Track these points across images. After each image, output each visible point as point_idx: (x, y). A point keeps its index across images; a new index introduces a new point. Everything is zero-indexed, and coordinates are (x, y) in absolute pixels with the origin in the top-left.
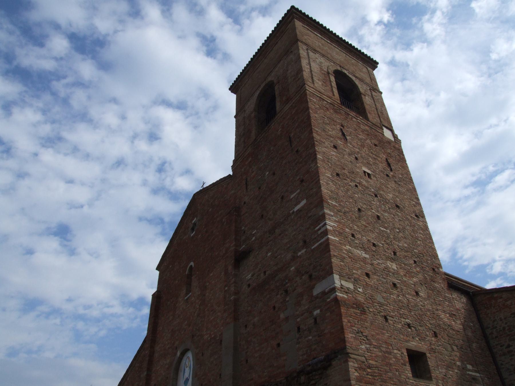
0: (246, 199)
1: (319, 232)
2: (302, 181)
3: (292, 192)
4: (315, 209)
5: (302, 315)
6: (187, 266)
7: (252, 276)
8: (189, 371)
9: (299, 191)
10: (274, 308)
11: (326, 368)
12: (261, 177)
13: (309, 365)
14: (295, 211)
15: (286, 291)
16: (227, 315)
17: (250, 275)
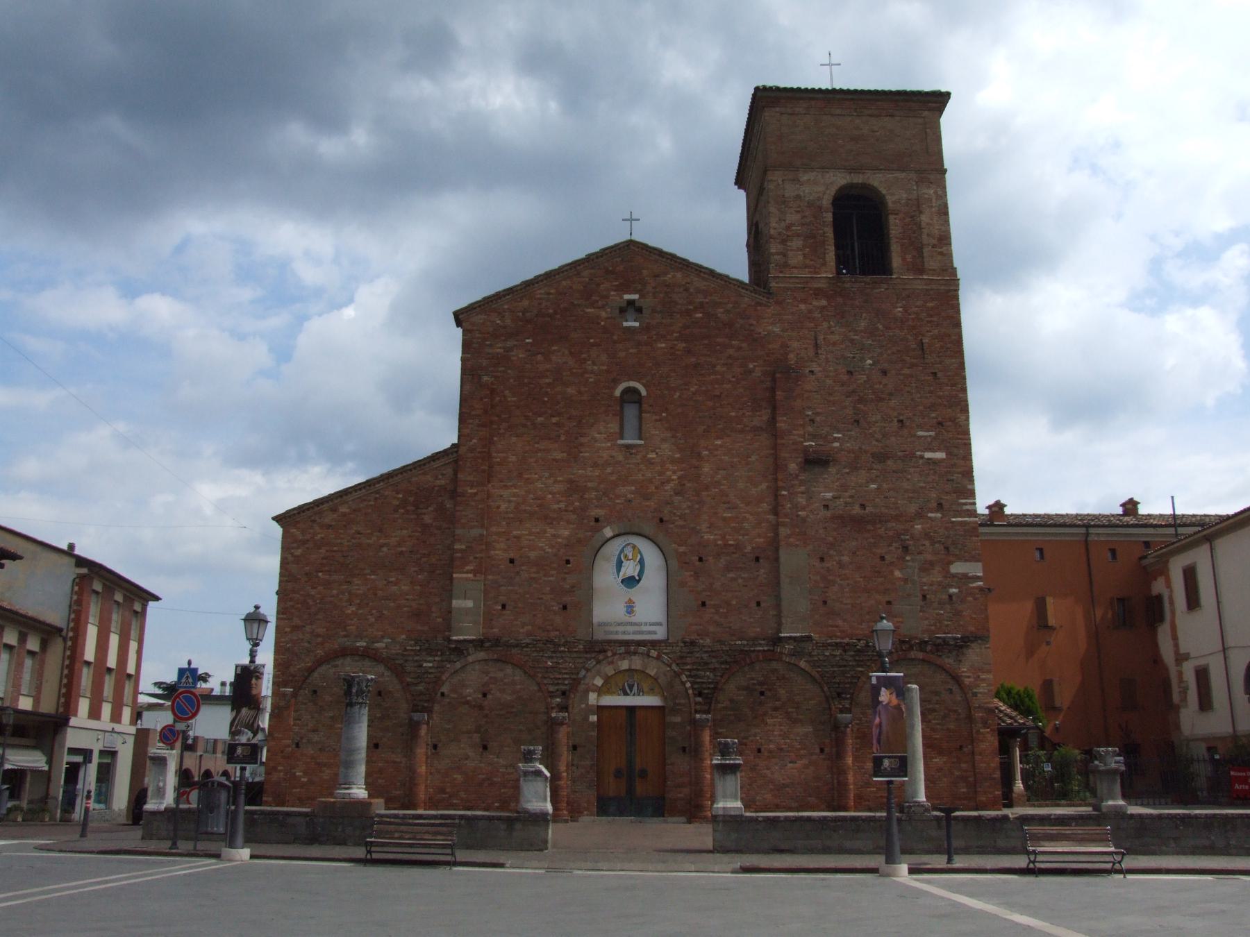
0: (816, 368)
3: (921, 427)
4: (960, 475)
5: (931, 585)
6: (616, 382)
7: (834, 498)
8: (638, 567)
9: (932, 433)
10: (882, 558)
11: (961, 647)
12: (854, 357)
14: (926, 457)
15: (906, 549)
16: (789, 532)
17: (831, 494)
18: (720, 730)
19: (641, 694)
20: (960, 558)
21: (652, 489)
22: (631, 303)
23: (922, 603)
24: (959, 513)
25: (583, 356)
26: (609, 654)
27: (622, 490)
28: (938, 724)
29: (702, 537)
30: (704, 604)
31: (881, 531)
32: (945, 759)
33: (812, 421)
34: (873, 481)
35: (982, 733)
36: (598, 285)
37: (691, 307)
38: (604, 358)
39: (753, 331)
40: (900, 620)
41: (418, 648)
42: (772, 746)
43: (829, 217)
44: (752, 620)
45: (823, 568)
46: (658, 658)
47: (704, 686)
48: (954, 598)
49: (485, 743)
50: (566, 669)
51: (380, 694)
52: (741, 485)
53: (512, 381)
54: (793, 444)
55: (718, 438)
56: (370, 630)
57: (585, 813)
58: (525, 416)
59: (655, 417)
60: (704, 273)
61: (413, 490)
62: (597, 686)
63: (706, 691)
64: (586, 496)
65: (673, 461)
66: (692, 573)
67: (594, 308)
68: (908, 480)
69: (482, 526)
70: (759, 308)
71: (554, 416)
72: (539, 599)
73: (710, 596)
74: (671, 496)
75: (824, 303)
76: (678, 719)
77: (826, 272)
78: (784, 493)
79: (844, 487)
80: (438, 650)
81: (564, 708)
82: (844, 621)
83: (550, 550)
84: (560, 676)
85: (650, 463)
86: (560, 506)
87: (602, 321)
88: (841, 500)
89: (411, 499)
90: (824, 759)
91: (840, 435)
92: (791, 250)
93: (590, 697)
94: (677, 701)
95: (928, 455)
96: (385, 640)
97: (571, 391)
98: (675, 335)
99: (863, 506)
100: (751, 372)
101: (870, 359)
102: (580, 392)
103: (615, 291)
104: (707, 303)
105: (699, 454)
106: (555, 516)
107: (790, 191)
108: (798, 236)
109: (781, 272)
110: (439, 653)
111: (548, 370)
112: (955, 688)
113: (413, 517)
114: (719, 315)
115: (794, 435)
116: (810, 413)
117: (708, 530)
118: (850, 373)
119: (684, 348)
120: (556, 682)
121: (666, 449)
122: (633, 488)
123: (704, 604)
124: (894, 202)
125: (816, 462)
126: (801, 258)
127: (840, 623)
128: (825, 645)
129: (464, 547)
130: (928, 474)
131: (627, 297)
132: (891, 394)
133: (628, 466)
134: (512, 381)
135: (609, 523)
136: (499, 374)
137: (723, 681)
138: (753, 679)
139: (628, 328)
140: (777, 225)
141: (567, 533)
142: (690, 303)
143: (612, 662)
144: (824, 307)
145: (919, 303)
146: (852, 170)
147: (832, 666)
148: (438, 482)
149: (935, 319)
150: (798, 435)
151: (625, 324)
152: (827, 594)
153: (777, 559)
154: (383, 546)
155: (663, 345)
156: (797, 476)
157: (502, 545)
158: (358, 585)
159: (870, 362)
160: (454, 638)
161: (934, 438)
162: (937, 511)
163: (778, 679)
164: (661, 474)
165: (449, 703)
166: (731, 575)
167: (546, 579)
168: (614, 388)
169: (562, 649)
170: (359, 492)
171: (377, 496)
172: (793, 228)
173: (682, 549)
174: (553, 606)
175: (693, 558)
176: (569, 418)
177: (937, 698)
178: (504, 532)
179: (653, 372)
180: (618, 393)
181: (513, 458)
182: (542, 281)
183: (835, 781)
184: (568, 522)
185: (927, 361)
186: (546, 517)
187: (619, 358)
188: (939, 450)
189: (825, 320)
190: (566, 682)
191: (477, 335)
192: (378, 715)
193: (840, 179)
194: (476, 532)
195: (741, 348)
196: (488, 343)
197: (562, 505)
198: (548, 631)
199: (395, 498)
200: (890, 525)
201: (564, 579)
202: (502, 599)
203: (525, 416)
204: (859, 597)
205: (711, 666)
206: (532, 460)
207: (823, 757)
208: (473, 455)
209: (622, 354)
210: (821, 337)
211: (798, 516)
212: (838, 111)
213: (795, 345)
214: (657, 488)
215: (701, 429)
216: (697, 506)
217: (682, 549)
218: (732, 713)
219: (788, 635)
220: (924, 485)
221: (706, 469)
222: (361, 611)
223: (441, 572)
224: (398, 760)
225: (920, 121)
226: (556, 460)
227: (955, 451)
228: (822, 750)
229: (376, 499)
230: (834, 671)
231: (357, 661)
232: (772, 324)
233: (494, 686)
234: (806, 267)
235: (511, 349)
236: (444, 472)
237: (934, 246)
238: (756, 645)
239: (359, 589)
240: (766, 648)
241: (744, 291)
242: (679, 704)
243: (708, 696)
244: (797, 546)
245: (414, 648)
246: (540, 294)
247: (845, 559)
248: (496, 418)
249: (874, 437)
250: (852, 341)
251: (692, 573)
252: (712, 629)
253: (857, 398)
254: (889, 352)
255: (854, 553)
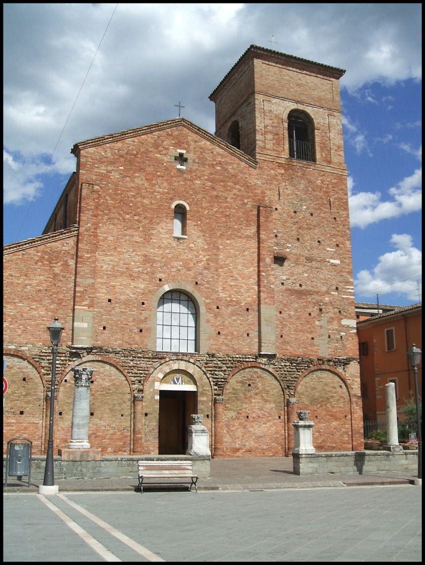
1: (349, 290)
2: (337, 245)
6: (172, 199)
10: (310, 314)
11: (347, 364)
13: (336, 358)
15: (321, 310)
18: (227, 406)
19: (183, 383)
20: (346, 317)
21: (191, 265)
22: (181, 155)
23: (329, 340)
24: (345, 293)
25: (154, 182)
26: (168, 359)
27: (175, 264)
28: (335, 404)
29: (219, 295)
30: (219, 333)
31: (309, 300)
32: (338, 422)
33: (276, 236)
34: (307, 272)
35: (356, 409)
36: (163, 142)
37: (215, 163)
38: (165, 184)
39: (246, 181)
40: (318, 348)
41: (50, 351)
42: (254, 415)
43: (286, 125)
44: (244, 344)
45: (281, 317)
46: (194, 364)
47: (219, 380)
48: (343, 338)
49: (92, 412)
50: (142, 367)
51: (24, 379)
52: (240, 267)
53: (111, 191)
54: (268, 247)
55: (228, 239)
56: (19, 338)
57: (152, 453)
58: (119, 213)
59: (194, 223)
60: (222, 145)
61: (47, 252)
62: (159, 378)
63: (220, 383)
64: (154, 265)
65: (204, 250)
66: (213, 315)
67: (161, 154)
68: (322, 273)
69: (94, 278)
70: (250, 169)
71: (136, 216)
72: (128, 325)
73: (221, 329)
74: (202, 270)
75: (283, 171)
76: (205, 399)
77: (284, 155)
78: (263, 274)
79: (292, 274)
80: (63, 353)
81: (141, 391)
82: (291, 347)
83: (132, 296)
84: (138, 372)
85: (191, 249)
86: (139, 270)
87: (165, 162)
88: (290, 280)
89: (46, 257)
90: (280, 422)
91: (290, 245)
92: (267, 140)
93: (156, 385)
94: (204, 388)
95: (332, 261)
96: (28, 345)
97: (146, 201)
98: (206, 177)
99: (301, 285)
100: (246, 204)
101: (305, 205)
102: (151, 203)
103: (172, 146)
104: (223, 162)
105: (218, 248)
106: (136, 275)
107: (267, 106)
108: (271, 132)
109: (262, 151)
110: (64, 355)
111: (132, 187)
112: (343, 385)
113: (47, 268)
114: (230, 170)
115: (269, 242)
116: (275, 231)
117: (222, 291)
118: (295, 212)
119: (210, 185)
120: (136, 375)
121: (200, 242)
122: (181, 263)
123: (219, 333)
124: (318, 123)
125: (279, 260)
126: (272, 145)
127: (289, 348)
128: (282, 360)
129: (82, 290)
130: (332, 272)
131: (179, 151)
132: (315, 226)
133: (179, 250)
134: (111, 191)
135: (167, 283)
136: (103, 186)
137: (230, 377)
138: (245, 377)
139: (179, 170)
140: (259, 124)
141: (143, 286)
142: (215, 160)
143: (169, 365)
144: (283, 174)
145: (329, 180)
146: (297, 102)
147: (285, 371)
148: (64, 248)
149: (336, 189)
150: (271, 243)
151: (179, 167)
152: (283, 332)
153: (259, 311)
154: (26, 286)
155: (199, 182)
156: (270, 265)
157: (104, 291)
158: (10, 309)
159: (305, 207)
160: (75, 346)
161: (335, 252)
162: (336, 292)
163: (258, 377)
164: (196, 256)
165: (70, 386)
166: (234, 318)
167: (130, 313)
168: (171, 204)
169: (140, 355)
170: (12, 249)
171: (24, 253)
172: (268, 128)
173: (208, 301)
174: (134, 330)
175: (214, 306)
176: (144, 218)
177: (334, 390)
178: (106, 283)
179: (193, 197)
180: (173, 206)
181: (111, 238)
182: (130, 133)
183: (287, 434)
184: (144, 280)
185: (332, 211)
186: (131, 276)
187: (175, 186)
188: (337, 259)
189: (283, 181)
190: (142, 376)
191: (90, 160)
192: (23, 393)
193: (293, 106)
194: (91, 281)
195: (241, 190)
196: (96, 165)
197: (140, 269)
198: (131, 344)
199: (35, 255)
200: (313, 296)
201: (141, 314)
202: (104, 323)
203: (119, 213)
204: (299, 334)
205: (223, 369)
206: (124, 240)
207: (280, 421)
208: (86, 233)
209: (176, 184)
210: (281, 191)
211: (270, 287)
212: (291, 69)
213: (268, 192)
214: (194, 264)
215: (219, 233)
216: (216, 277)
217: (208, 301)
218: (234, 396)
219: (265, 353)
220: (329, 276)
221: (221, 257)
222: (12, 326)
223: (65, 304)
224: (36, 422)
225: (331, 82)
226: (137, 242)
227: (345, 260)
228: (279, 417)
229: (23, 254)
230: (286, 374)
231: (9, 358)
232: (257, 179)
233: (98, 376)
234: (274, 150)
235: (110, 172)
236: (68, 242)
237: (336, 150)
238: (246, 358)
239: (10, 312)
240: (251, 360)
241: (243, 158)
242: (205, 390)
243: (220, 385)
244: (270, 304)
245: (47, 351)
246: (129, 141)
247: (292, 313)
248: (102, 213)
249: (306, 248)
250: (296, 195)
251: (213, 315)
252: (223, 348)
253: (298, 226)
254: (314, 203)
255: (296, 310)
